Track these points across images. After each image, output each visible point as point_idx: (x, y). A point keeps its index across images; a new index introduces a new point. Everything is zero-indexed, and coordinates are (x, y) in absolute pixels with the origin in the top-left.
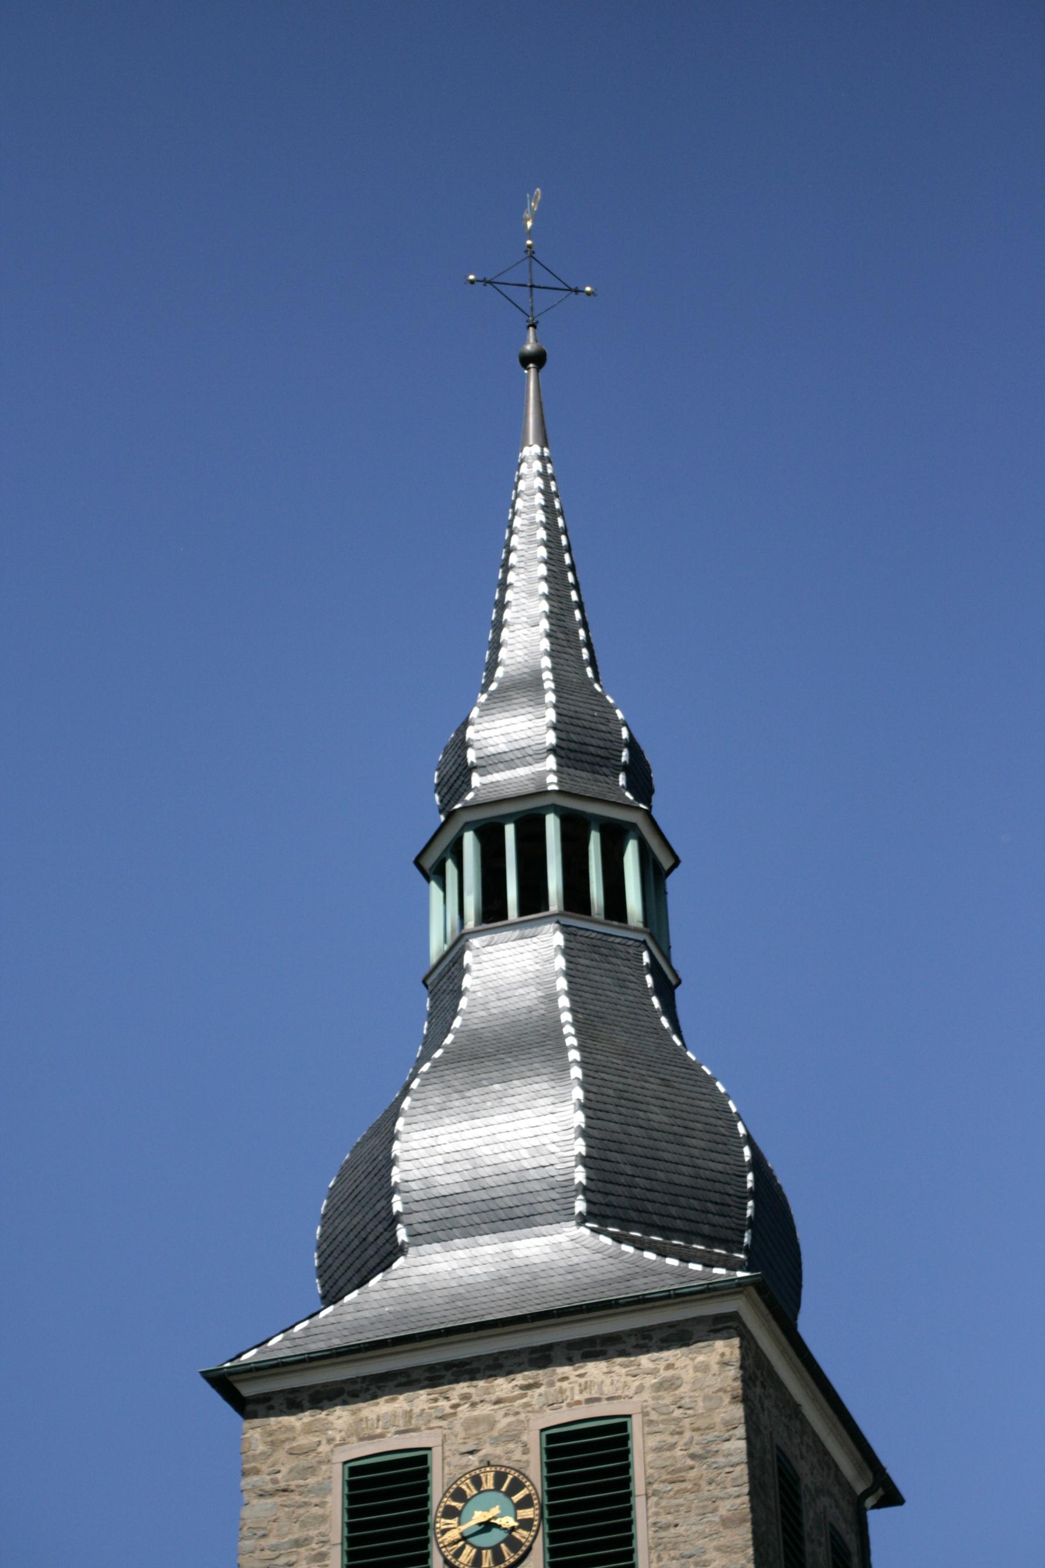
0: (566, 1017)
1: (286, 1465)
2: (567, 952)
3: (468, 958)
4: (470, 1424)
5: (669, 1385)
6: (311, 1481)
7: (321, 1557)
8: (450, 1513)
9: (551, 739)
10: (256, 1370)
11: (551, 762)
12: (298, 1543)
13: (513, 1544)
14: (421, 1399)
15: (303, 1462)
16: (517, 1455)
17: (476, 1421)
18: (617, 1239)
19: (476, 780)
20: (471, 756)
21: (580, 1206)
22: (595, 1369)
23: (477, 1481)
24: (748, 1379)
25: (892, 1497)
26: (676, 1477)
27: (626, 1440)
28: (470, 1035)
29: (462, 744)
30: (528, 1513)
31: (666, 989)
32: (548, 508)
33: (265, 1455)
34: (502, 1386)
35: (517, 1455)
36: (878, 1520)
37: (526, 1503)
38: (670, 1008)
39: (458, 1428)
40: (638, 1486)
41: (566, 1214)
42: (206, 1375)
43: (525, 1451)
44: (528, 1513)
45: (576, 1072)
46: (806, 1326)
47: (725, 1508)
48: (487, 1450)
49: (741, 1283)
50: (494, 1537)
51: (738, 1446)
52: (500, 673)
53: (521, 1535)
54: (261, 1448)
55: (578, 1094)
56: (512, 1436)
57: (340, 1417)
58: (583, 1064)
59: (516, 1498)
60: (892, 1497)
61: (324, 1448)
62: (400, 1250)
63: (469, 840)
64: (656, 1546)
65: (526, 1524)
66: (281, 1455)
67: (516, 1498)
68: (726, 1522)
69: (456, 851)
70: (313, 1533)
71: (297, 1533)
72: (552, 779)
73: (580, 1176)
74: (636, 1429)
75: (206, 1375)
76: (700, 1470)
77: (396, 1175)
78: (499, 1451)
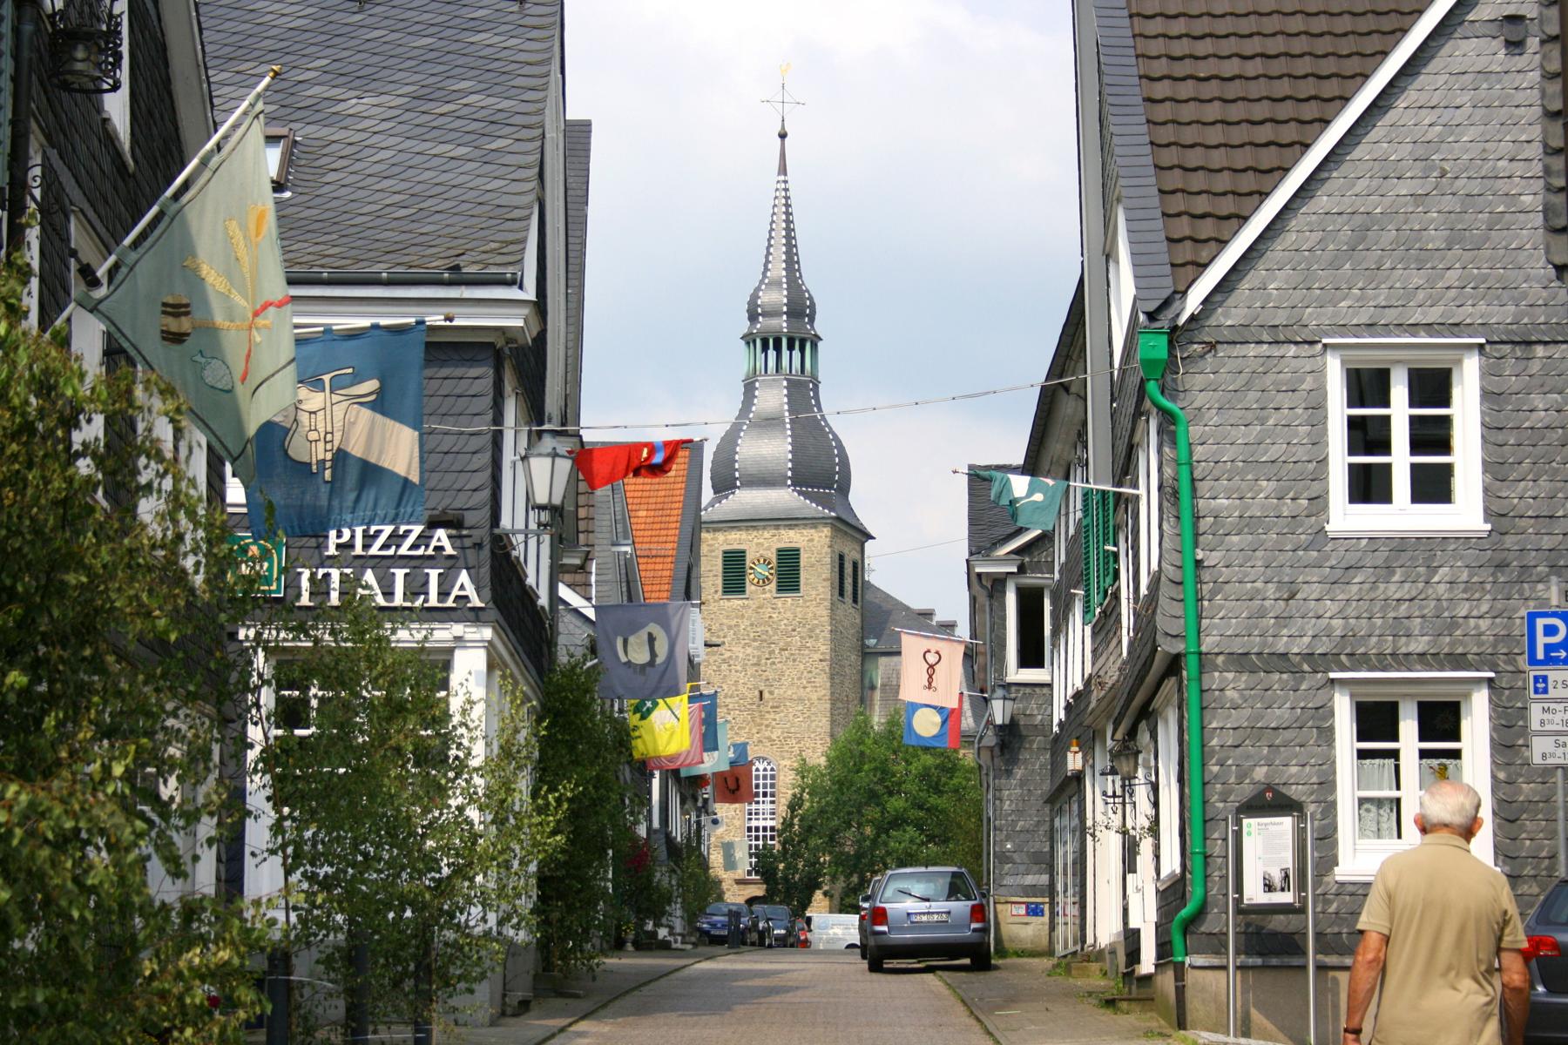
4: (757, 544)
5: (812, 540)
11: (785, 317)
18: (800, 493)
19: (761, 319)
21: (789, 482)
31: (816, 387)
40: (802, 564)
41: (784, 485)
45: (789, 433)
47: (824, 576)
49: (832, 518)
52: (769, 274)
55: (790, 440)
56: (768, 549)
57: (721, 537)
58: (791, 429)
63: (758, 342)
64: (806, 584)
72: (785, 325)
73: (789, 474)
74: (802, 551)
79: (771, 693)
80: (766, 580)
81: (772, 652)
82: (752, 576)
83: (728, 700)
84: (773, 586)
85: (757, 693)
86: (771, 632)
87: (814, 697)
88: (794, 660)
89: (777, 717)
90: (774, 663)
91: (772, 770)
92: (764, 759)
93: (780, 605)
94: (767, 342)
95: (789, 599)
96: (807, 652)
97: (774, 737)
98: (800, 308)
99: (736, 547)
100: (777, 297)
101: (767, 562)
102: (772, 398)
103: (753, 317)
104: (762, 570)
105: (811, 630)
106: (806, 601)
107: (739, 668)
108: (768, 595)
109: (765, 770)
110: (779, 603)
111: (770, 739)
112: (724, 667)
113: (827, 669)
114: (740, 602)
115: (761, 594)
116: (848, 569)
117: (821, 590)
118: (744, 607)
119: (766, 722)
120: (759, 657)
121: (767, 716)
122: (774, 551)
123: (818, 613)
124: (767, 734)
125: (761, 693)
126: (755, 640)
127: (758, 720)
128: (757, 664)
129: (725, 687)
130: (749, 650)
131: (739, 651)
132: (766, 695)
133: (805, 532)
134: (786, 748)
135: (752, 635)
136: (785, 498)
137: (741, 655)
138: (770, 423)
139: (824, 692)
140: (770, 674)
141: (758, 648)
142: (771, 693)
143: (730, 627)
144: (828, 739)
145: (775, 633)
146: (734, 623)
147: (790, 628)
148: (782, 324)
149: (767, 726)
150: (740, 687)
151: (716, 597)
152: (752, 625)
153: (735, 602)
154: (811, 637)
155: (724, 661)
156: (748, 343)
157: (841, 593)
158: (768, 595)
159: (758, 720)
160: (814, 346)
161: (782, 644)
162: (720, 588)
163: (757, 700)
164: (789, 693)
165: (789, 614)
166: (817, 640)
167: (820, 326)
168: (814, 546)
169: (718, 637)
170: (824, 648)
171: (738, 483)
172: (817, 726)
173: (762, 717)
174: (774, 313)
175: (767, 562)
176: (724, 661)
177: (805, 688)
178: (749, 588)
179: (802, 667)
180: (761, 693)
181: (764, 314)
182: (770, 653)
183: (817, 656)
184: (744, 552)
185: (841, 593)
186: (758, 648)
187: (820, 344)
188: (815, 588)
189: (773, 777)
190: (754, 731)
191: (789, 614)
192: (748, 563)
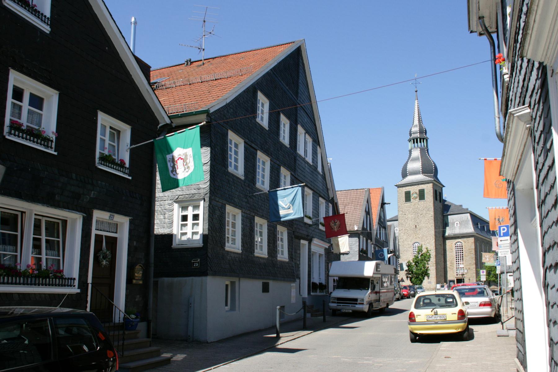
0: (420, 157)
1: (400, 191)
2: (420, 150)
3: (412, 151)
5: (427, 187)
9: (418, 131)
10: (398, 185)
11: (418, 133)
14: (410, 187)
18: (424, 175)
19: (412, 135)
20: (412, 133)
21: (421, 173)
22: (422, 185)
24: (433, 185)
25: (444, 186)
26: (428, 193)
28: (413, 158)
29: (410, 131)
31: (427, 150)
32: (418, 107)
34: (416, 186)
36: (443, 188)
38: (428, 152)
45: (421, 161)
46: (439, 177)
51: (432, 191)
57: (404, 188)
60: (444, 186)
62: (407, 176)
63: (412, 140)
69: (411, 141)
72: (419, 135)
73: (421, 171)
76: (429, 193)
77: (407, 170)
79: (418, 226)
80: (416, 198)
81: (418, 215)
83: (407, 228)
84: (418, 199)
85: (415, 226)
87: (430, 226)
92: (417, 242)
94: (415, 140)
95: (422, 202)
96: (427, 215)
97: (420, 237)
98: (423, 131)
100: (416, 129)
101: (416, 193)
102: (416, 153)
103: (411, 135)
104: (415, 195)
107: (410, 220)
108: (417, 201)
110: (420, 203)
111: (419, 237)
112: (406, 220)
113: (433, 219)
115: (415, 201)
116: (438, 194)
118: (411, 205)
122: (418, 191)
124: (418, 236)
125: (416, 226)
126: (414, 213)
127: (415, 233)
128: (415, 219)
130: (412, 215)
131: (410, 216)
132: (417, 226)
133: (426, 185)
136: (421, 177)
137: (410, 217)
138: (416, 159)
139: (432, 224)
140: (418, 221)
142: (418, 226)
143: (407, 210)
145: (419, 211)
146: (408, 209)
148: (418, 135)
151: (404, 203)
152: (413, 209)
153: (408, 204)
156: (409, 142)
158: (417, 201)
159: (415, 233)
160: (427, 141)
161: (421, 213)
162: (404, 201)
163: (415, 227)
165: (422, 206)
166: (430, 211)
167: (428, 135)
168: (429, 189)
170: (432, 213)
171: (408, 175)
173: (416, 232)
174: (416, 133)
175: (416, 193)
178: (412, 200)
180: (416, 226)
181: (413, 133)
184: (410, 191)
185: (436, 199)
187: (428, 140)
188: (429, 198)
191: (422, 206)
192: (411, 194)
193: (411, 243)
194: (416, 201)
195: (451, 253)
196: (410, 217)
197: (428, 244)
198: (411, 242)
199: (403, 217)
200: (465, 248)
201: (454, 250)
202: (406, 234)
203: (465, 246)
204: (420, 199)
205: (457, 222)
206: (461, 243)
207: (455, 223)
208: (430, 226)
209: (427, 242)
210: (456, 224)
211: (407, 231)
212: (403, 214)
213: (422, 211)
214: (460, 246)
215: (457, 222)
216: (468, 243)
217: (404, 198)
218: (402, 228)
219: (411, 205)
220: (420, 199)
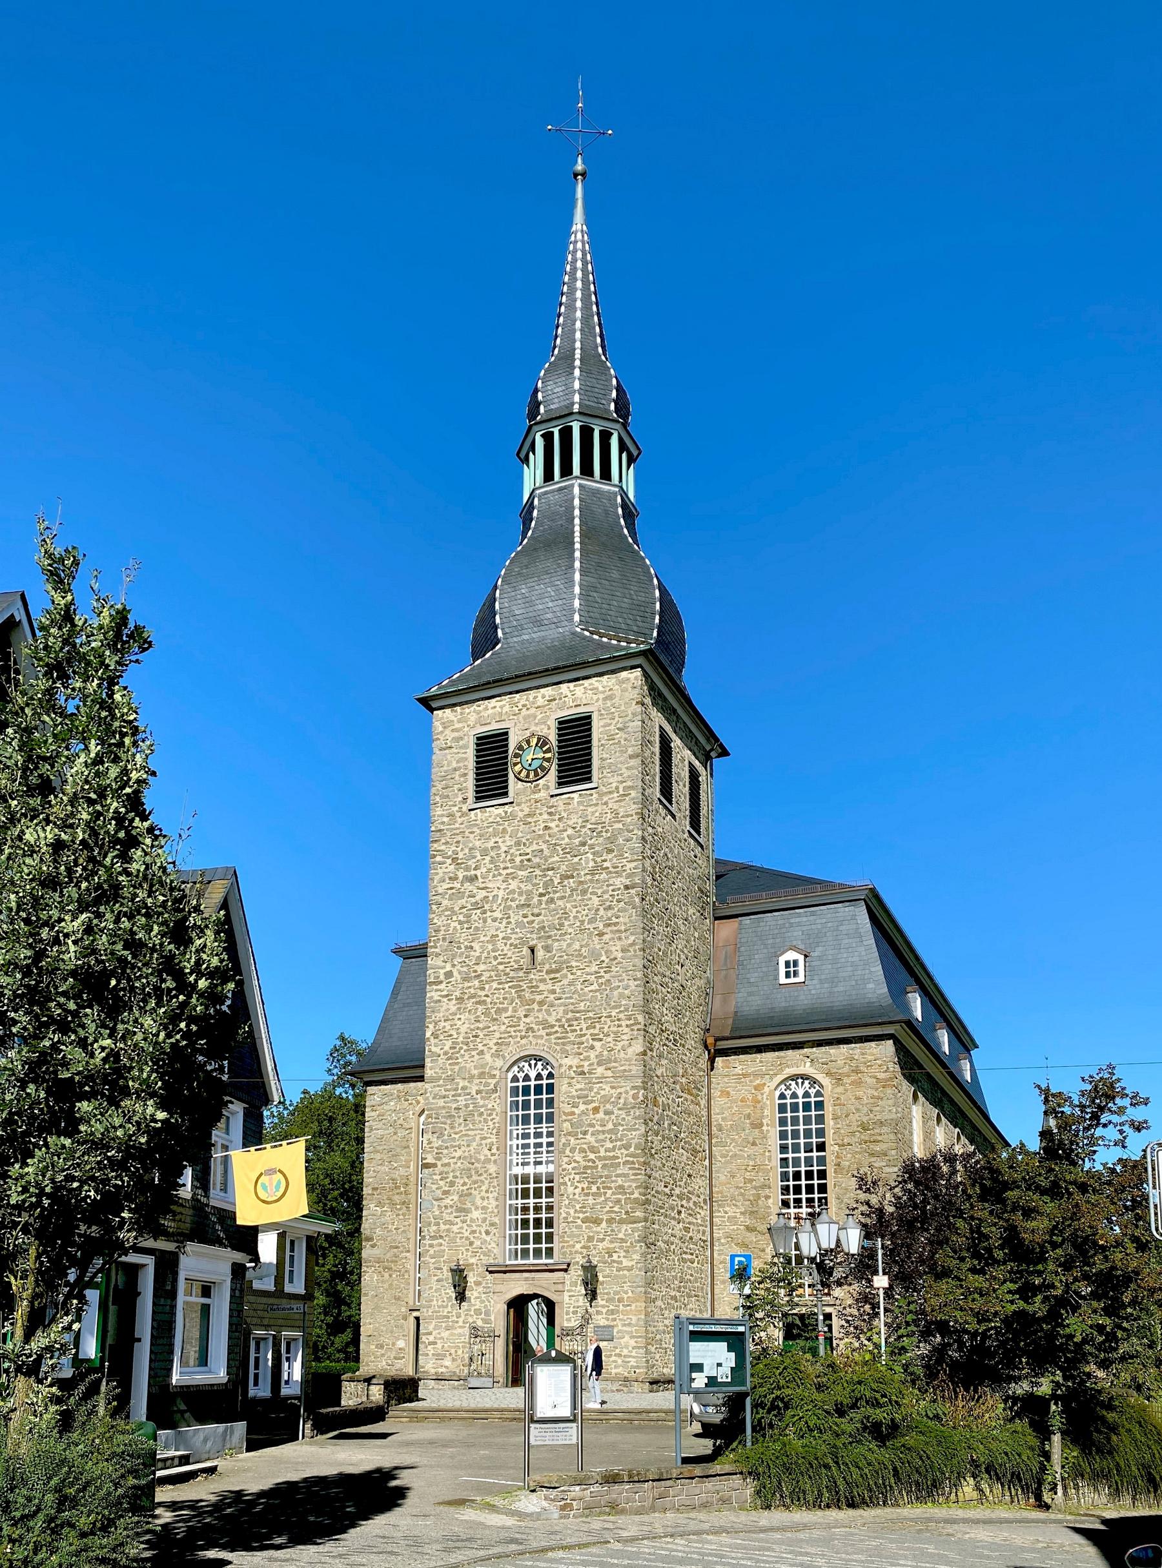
6: (461, 743)
7: (465, 775)
8: (516, 756)
12: (455, 770)
13: (541, 767)
15: (456, 734)
16: (546, 731)
17: (529, 716)
23: (528, 742)
25: (724, 753)
27: (590, 723)
30: (548, 755)
33: (442, 732)
35: (546, 731)
37: (548, 751)
39: (521, 719)
42: (418, 700)
43: (549, 729)
44: (548, 755)
47: (630, 751)
48: (533, 728)
50: (536, 764)
53: (546, 764)
54: (441, 729)
59: (544, 749)
60: (724, 753)
61: (466, 729)
64: (601, 768)
65: (548, 760)
66: (447, 732)
67: (544, 749)
68: (631, 757)
70: (461, 764)
71: (454, 765)
75: (418, 700)
78: (538, 729)
79: (547, 949)
82: (518, 768)
83: (482, 967)
85: (526, 951)
86: (546, 852)
88: (584, 892)
89: (557, 987)
90: (552, 900)
91: (550, 1076)
92: (538, 1059)
93: (561, 808)
95: (576, 794)
96: (604, 876)
97: (551, 1020)
99: (494, 727)
105: (612, 840)
106: (601, 795)
107: (498, 914)
109: (539, 1077)
110: (559, 802)
111: (546, 1025)
114: (501, 810)
117: (626, 773)
118: (507, 818)
119: (538, 998)
120: (529, 893)
121: (542, 987)
122: (553, 725)
123: (622, 812)
126: (522, 867)
129: (476, 945)
130: (514, 885)
132: (540, 954)
134: (572, 1037)
135: (518, 859)
137: (501, 893)
139: (632, 938)
141: (528, 879)
142: (547, 949)
143: (485, 852)
144: (640, 1018)
146: (491, 844)
147: (577, 841)
149: (541, 1003)
150: (500, 945)
151: (465, 808)
152: (518, 844)
153: (493, 811)
154: (610, 851)
155: (476, 907)
157: (666, 790)
158: (543, 794)
162: (471, 794)
163: (525, 962)
164: (577, 946)
165: (575, 819)
169: (467, 869)
172: (621, 995)
173: (534, 989)
175: (543, 742)
176: (476, 907)
177: (601, 934)
179: (594, 897)
182: (546, 885)
183: (619, 882)
185: (666, 790)
186: (528, 879)
189: (550, 1089)
190: (521, 1013)
193: (499, 1063)
194: (537, 790)
195: (749, 1150)
196: (501, 893)
197: (600, 1070)
198: (497, 1055)
199: (460, 894)
200: (836, 1118)
201: (773, 1133)
202: (470, 1004)
203: (837, 1102)
204: (564, 780)
205: (791, 956)
206: (814, 1082)
207: (782, 960)
208: (616, 950)
209: (592, 1054)
210: (782, 970)
211: (476, 983)
212: (460, 875)
213: (570, 851)
214: (806, 1107)
215: (791, 956)
216: (858, 1083)
217: (471, 776)
218: (448, 968)
219: (507, 818)
220: (564, 780)
